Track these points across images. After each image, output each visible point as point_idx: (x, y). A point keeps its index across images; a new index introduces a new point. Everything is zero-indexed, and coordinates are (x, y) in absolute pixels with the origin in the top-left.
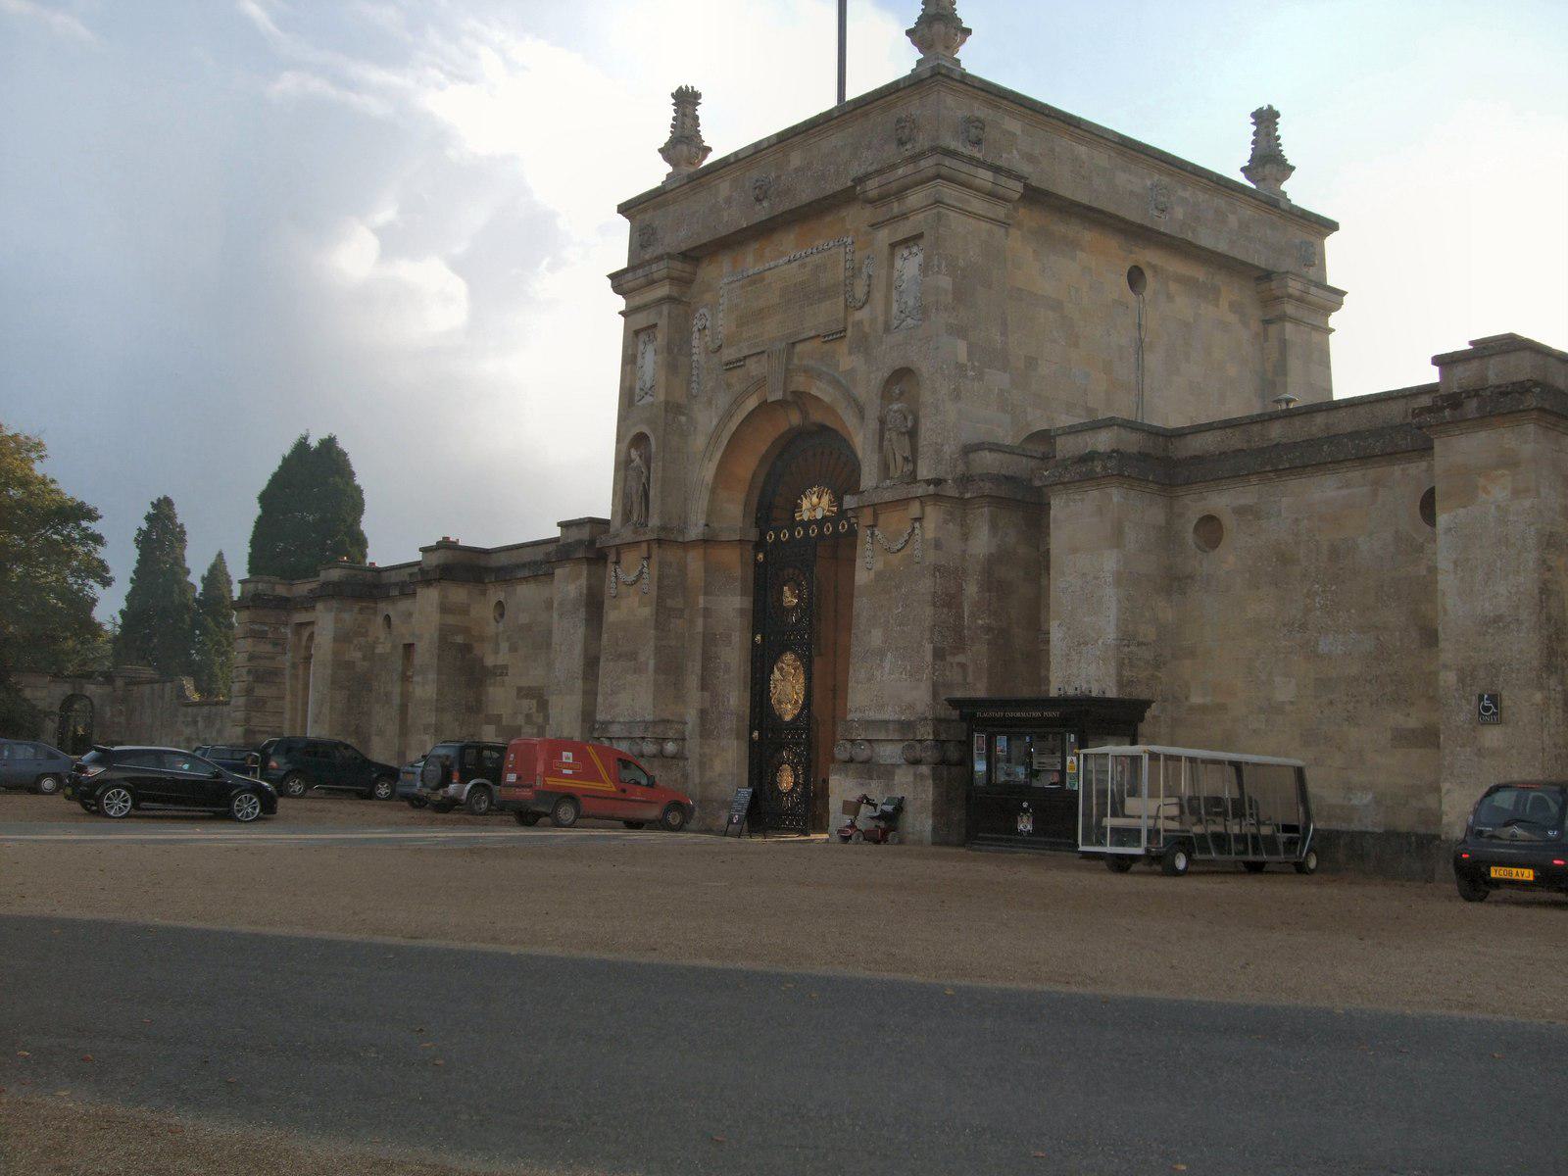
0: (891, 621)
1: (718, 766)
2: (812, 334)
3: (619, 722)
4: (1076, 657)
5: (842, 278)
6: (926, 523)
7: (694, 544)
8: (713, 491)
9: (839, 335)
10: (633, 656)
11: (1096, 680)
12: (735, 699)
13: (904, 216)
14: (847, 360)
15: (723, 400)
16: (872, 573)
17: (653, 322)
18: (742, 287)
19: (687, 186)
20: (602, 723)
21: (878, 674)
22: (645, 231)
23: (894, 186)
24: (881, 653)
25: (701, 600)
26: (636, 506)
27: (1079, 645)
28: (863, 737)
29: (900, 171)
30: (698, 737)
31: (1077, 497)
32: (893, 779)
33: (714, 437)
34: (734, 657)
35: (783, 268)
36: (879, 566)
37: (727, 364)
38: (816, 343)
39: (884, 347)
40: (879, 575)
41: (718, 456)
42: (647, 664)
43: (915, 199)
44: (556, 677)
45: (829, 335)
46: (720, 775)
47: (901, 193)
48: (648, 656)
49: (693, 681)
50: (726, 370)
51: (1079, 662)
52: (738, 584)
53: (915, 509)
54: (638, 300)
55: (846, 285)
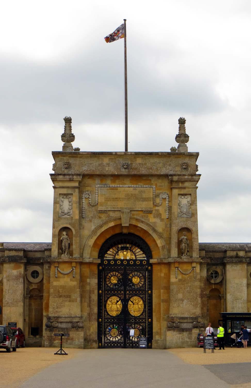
0: (185, 292)
1: (92, 330)
2: (140, 209)
3: (63, 317)
4: (236, 302)
5: (152, 196)
6: (196, 268)
7: (86, 263)
8: (92, 247)
9: (150, 212)
10: (69, 296)
11: (241, 308)
12: (96, 310)
13: (185, 188)
14: (152, 219)
15: (97, 222)
16: (177, 280)
17: (72, 193)
18: (107, 189)
19: (89, 155)
20: (54, 317)
21: (181, 305)
22: (68, 164)
23: (183, 180)
24: (182, 300)
25: (88, 280)
26: (67, 250)
27: (236, 299)
28: (178, 321)
29: (186, 177)
30: (88, 321)
31: (235, 266)
32: (192, 332)
33: (94, 232)
34: (95, 297)
35: (126, 188)
36: (180, 277)
37: (100, 211)
38: (140, 212)
39: (178, 221)
40: (180, 280)
41: (95, 238)
42: (77, 299)
43: (187, 184)
44: (6, 301)
45: (149, 211)
46: (92, 332)
47: (183, 182)
48: (76, 296)
49: (86, 304)
50: (99, 213)
51: (236, 303)
52: (97, 276)
53: (194, 265)
54: (61, 184)
55: (153, 199)
